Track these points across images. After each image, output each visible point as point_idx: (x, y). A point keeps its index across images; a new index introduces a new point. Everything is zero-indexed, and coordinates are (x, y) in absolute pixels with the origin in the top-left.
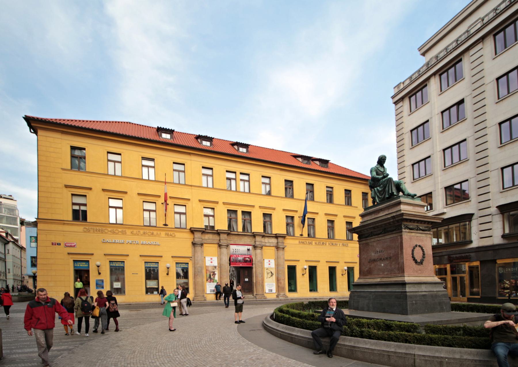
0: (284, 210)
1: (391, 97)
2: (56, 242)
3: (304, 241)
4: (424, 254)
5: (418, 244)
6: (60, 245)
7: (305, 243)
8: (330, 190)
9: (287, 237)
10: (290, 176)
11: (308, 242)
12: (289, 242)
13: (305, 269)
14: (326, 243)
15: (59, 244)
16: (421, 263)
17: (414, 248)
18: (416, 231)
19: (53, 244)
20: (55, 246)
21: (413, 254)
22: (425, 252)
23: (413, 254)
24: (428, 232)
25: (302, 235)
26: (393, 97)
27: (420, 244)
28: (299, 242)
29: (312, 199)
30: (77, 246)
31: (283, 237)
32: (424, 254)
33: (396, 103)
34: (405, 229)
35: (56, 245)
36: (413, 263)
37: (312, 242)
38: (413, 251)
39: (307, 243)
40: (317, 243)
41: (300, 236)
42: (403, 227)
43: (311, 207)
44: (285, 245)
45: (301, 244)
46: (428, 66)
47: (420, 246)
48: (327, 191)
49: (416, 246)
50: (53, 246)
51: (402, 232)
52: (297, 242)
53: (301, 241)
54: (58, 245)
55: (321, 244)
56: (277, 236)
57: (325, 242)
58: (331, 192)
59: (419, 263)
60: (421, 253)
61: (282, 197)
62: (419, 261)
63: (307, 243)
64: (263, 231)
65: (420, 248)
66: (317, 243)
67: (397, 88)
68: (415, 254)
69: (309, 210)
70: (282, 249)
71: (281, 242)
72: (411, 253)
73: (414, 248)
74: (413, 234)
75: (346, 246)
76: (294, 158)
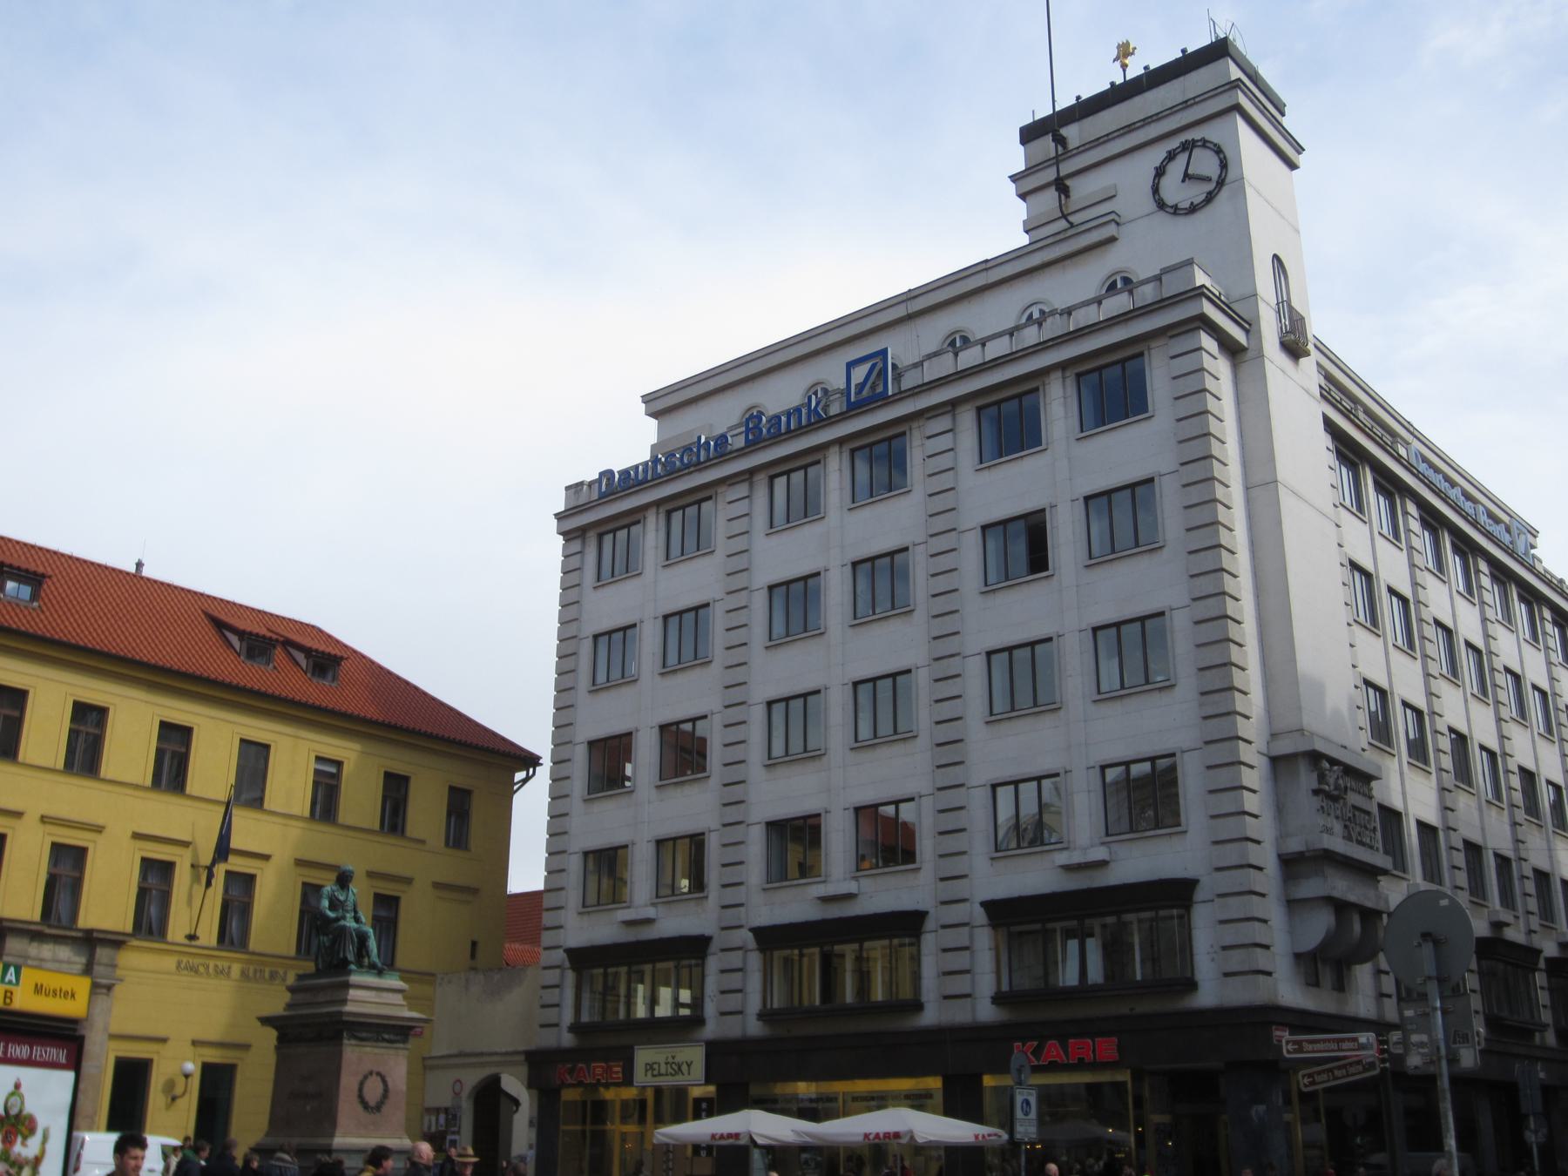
0: (137, 836)
3: (197, 961)
4: (386, 1090)
5: (376, 1069)
7: (202, 969)
8: (333, 770)
9: (135, 943)
10: (181, 711)
11: (216, 966)
12: (137, 961)
13: (187, 1076)
14: (285, 973)
16: (378, 1108)
17: (366, 1077)
18: (374, 1044)
21: (360, 1090)
22: (390, 1084)
23: (360, 1090)
24: (401, 1045)
25: (192, 937)
26: (560, 517)
27: (381, 1070)
28: (179, 966)
29: (257, 803)
31: (116, 942)
32: (386, 1090)
33: (568, 535)
34: (349, 1040)
36: (360, 1108)
37: (229, 968)
38: (362, 1084)
39: (211, 970)
40: (251, 974)
41: (186, 942)
42: (345, 1034)
43: (249, 831)
44: (119, 973)
45: (186, 972)
47: (379, 1074)
48: (317, 772)
49: (371, 1073)
51: (341, 1045)
52: (169, 962)
53: (185, 960)
55: (267, 975)
56: (91, 941)
57: (281, 972)
58: (332, 775)
59: (372, 1108)
60: (381, 1086)
61: (136, 787)
62: (372, 1103)
63: (211, 970)
64: (37, 916)
65: (379, 1079)
66: (251, 974)
67: (573, 490)
68: (366, 1090)
69: (236, 842)
70: (104, 991)
71: (105, 960)
72: (356, 1087)
73: (366, 1077)
74: (368, 1049)
76: (210, 633)
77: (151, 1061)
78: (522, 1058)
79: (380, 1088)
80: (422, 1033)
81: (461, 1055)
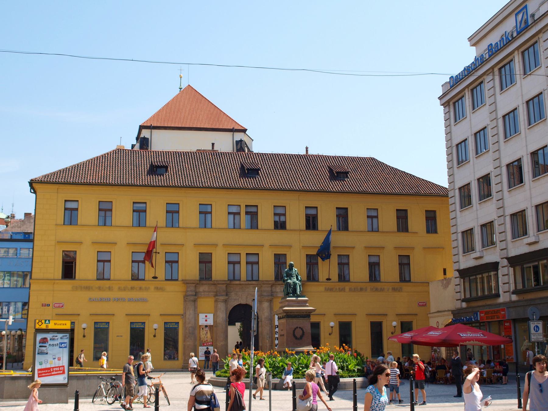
1: (438, 98)
2: (45, 303)
6: (49, 306)
15: (48, 305)
19: (42, 306)
20: (45, 307)
22: (305, 331)
30: (64, 307)
35: (45, 306)
37: (344, 288)
46: (480, 62)
47: (300, 328)
49: (297, 328)
50: (43, 307)
54: (47, 306)
72: (292, 332)
73: (295, 329)
75: (400, 290)
77: (351, 322)
78: (450, 313)
79: (301, 332)
80: (426, 305)
81: (438, 312)
